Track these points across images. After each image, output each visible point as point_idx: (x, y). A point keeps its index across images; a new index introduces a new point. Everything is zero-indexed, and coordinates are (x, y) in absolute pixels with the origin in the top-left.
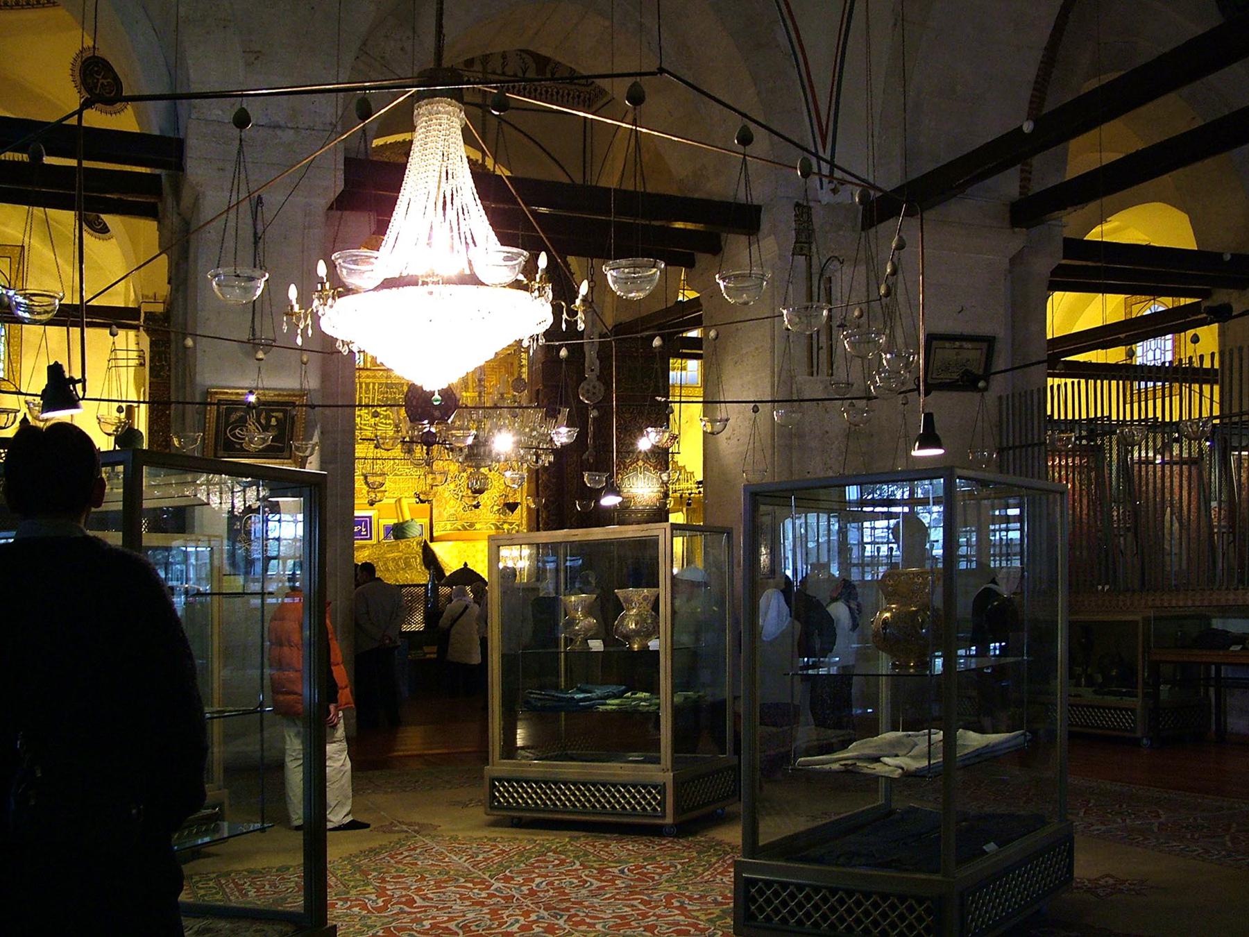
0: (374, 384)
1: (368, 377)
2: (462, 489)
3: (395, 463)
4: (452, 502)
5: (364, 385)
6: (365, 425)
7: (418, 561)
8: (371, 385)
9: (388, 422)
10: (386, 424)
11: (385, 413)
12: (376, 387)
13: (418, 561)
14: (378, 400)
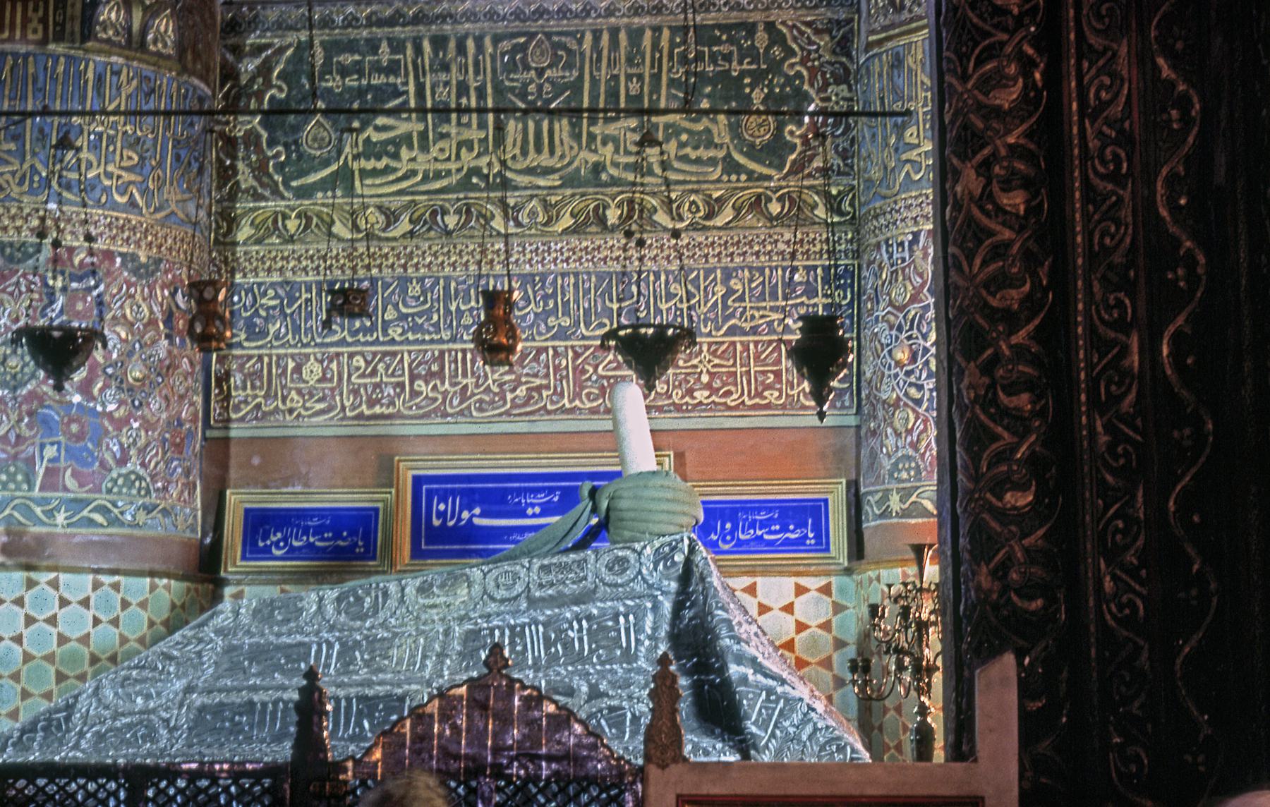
0: (657, 29)
3: (730, 292)
5: (623, 36)
8: (648, 34)
10: (698, 161)
12: (664, 43)
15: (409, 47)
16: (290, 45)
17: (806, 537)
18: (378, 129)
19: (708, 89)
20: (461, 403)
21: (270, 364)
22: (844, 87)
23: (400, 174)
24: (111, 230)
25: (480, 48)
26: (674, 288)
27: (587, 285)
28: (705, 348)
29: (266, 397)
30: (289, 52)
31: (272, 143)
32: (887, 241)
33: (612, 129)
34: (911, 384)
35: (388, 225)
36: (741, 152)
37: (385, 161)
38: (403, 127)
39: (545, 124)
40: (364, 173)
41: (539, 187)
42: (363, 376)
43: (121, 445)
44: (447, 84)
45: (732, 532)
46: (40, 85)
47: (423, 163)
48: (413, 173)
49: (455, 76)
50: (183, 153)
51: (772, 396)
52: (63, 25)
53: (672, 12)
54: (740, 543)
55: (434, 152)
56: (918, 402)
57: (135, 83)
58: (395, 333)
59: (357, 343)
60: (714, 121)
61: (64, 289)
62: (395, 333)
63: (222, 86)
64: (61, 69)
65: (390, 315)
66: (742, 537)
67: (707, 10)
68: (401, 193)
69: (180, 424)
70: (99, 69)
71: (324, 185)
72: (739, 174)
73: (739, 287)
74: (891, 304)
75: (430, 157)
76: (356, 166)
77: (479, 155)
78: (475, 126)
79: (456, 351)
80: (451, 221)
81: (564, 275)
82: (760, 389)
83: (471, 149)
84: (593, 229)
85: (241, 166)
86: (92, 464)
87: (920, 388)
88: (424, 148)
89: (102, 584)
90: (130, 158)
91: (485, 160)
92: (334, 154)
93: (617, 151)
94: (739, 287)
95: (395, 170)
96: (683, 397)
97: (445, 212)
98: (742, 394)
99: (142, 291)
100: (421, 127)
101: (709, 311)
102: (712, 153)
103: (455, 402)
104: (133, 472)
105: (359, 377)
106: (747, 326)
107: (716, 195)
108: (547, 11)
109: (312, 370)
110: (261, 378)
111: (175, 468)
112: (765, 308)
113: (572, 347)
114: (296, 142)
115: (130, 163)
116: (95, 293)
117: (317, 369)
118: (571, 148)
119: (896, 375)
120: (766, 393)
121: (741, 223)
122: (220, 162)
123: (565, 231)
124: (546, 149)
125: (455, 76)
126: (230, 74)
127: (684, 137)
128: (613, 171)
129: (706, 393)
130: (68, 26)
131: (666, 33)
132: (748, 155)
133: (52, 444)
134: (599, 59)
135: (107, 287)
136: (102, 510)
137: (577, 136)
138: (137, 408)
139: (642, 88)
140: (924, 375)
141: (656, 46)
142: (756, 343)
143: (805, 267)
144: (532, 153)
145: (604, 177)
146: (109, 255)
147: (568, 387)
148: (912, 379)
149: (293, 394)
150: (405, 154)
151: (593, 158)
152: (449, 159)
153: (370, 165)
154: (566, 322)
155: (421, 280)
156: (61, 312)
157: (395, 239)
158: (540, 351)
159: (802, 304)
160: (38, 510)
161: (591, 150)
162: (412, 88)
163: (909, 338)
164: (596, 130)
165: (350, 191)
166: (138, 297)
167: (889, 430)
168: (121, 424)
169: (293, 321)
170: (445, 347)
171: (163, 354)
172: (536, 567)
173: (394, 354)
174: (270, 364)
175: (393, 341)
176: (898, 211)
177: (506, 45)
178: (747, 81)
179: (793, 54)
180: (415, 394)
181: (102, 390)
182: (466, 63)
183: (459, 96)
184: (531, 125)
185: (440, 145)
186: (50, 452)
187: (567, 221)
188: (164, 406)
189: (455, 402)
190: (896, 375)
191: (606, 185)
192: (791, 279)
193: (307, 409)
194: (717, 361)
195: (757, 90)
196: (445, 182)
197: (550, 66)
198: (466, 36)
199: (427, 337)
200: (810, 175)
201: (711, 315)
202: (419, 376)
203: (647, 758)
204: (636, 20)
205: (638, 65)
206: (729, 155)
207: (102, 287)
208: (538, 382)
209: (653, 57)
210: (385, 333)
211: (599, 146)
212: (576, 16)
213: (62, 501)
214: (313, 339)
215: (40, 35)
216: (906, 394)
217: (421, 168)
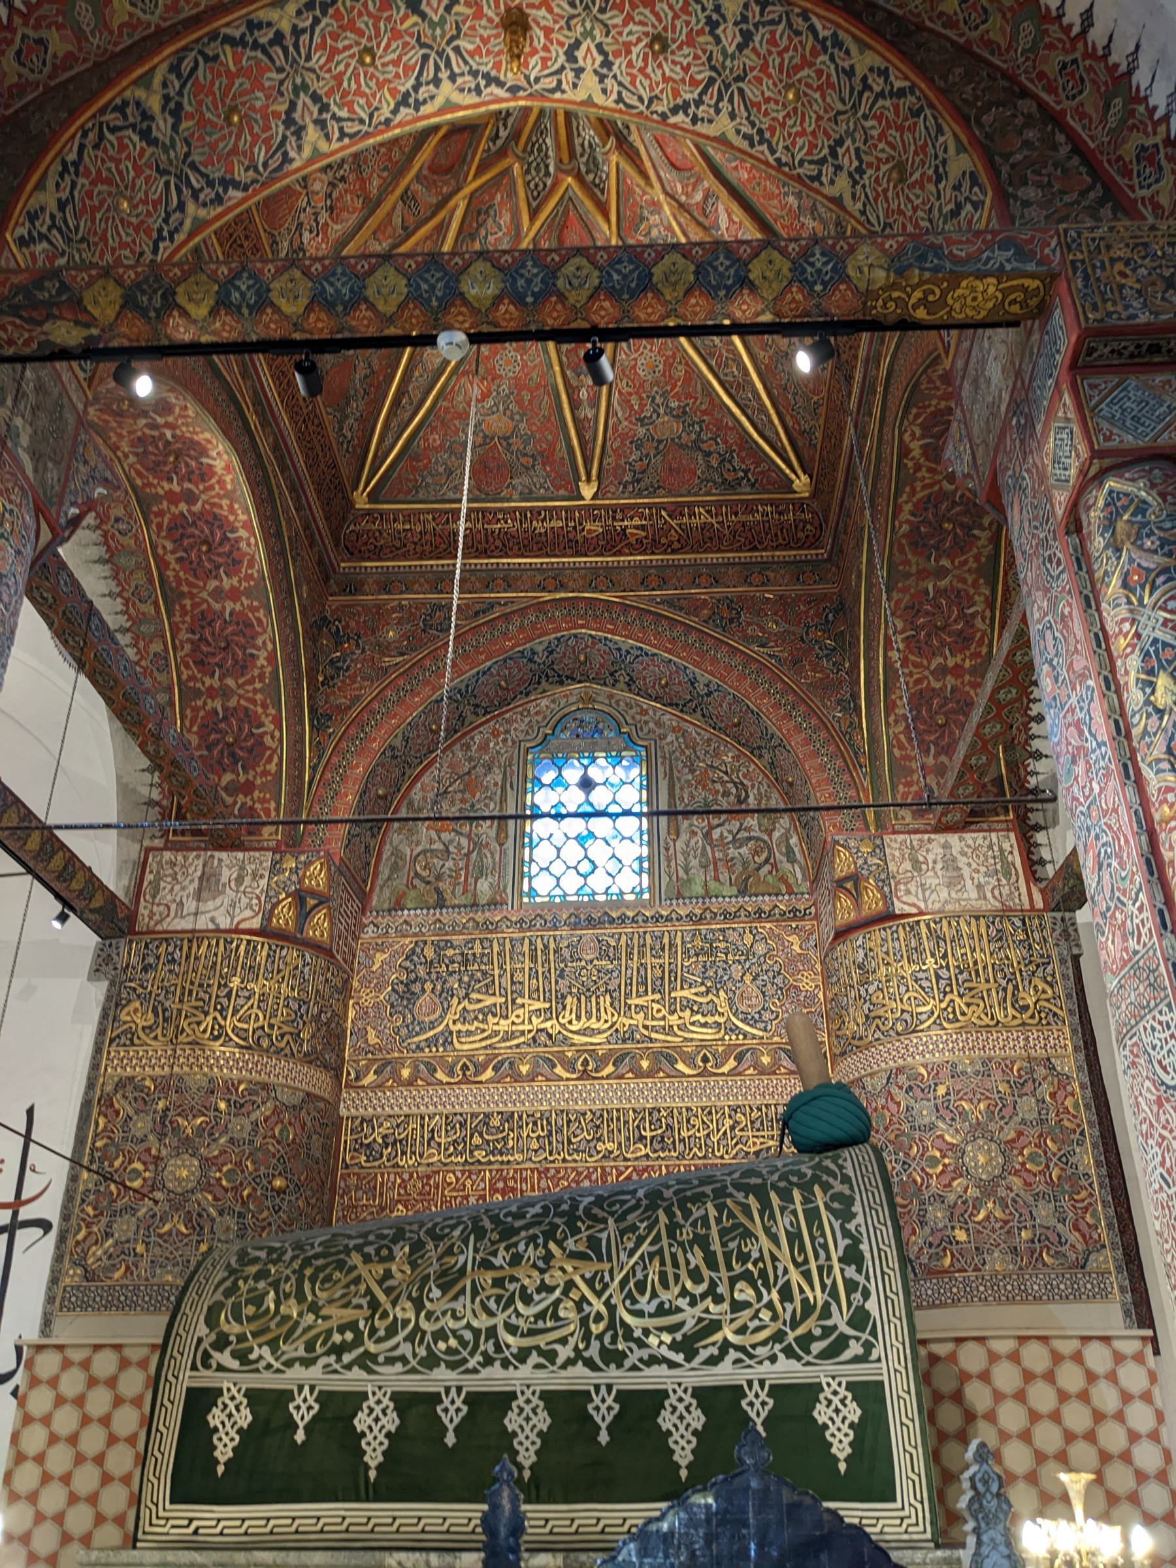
9: (710, 1020)
10: (705, 1025)
38: (489, 1001)
42: (454, 1190)
47: (504, 1025)
55: (513, 1018)
65: (477, 1140)
68: (485, 1048)
77: (546, 1020)
95: (484, 1031)
102: (717, 1018)
123: (608, 1077)
132: (744, 1021)
144: (583, 1019)
151: (628, 1022)
153: (467, 1027)
206: (729, 1019)
210: (472, 1156)
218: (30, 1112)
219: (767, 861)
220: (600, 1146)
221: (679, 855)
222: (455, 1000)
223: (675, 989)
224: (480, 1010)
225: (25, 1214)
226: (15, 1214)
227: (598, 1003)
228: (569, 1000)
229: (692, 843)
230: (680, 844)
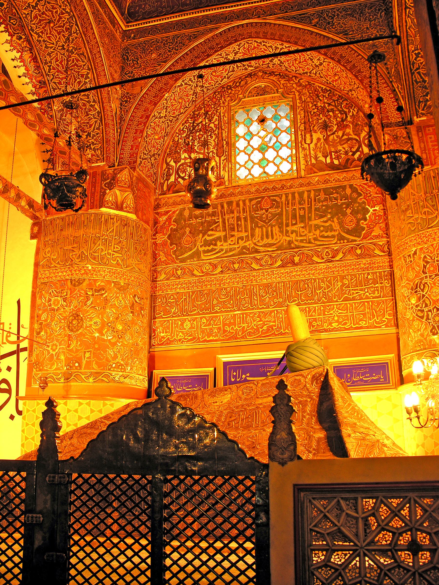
0: (309, 191)
1: (301, 185)
2: (428, 302)
4: (416, 323)
6: (302, 241)
7: (308, 409)
8: (306, 193)
11: (327, 224)
12: (312, 195)
13: (308, 409)
14: (316, 209)
15: (219, 206)
16: (177, 210)
17: (380, 378)
18: (209, 236)
19: (330, 211)
20: (242, 334)
21: (172, 323)
22: (381, 205)
23: (217, 251)
24: (110, 273)
25: (244, 204)
26: (322, 285)
27: (288, 286)
28: (335, 307)
29: (171, 335)
30: (177, 212)
31: (171, 245)
32: (403, 256)
33: (294, 228)
34: (419, 310)
35: (213, 269)
36: (344, 232)
37: (212, 246)
38: (218, 234)
39: (270, 229)
40: (205, 252)
41: (269, 251)
43: (114, 352)
44: (233, 217)
45: (350, 378)
46: (85, 224)
47: (226, 246)
48: (222, 250)
49: (236, 214)
50: (138, 247)
51: (363, 323)
52: (93, 203)
53: (314, 185)
54: (354, 382)
55: (229, 242)
56: (422, 317)
57: (119, 222)
58: (217, 309)
59: (204, 314)
60: (333, 221)
61: (93, 295)
62: (217, 309)
63: (154, 226)
64: (92, 218)
65: (215, 302)
66: (354, 379)
67: (327, 183)
68: (217, 258)
69: (138, 345)
70: (106, 218)
71: (191, 257)
72: (343, 240)
73: (347, 282)
74: (407, 280)
75: (228, 244)
76: (201, 249)
77: (245, 242)
78: (244, 231)
79: (240, 314)
80: (236, 266)
81: (279, 283)
82: (358, 321)
83: (243, 240)
84: (289, 265)
85: (161, 253)
86: (103, 359)
87: (422, 311)
88: (226, 241)
89: (107, 404)
90: (117, 248)
91: (248, 243)
92: (194, 246)
93: (297, 236)
94: (347, 282)
95: (215, 249)
96: (328, 326)
97: (234, 263)
98: (351, 323)
99: (122, 295)
100: (224, 233)
101: (336, 292)
102: (333, 233)
103: (240, 333)
104: (118, 362)
105: (204, 326)
106: (351, 297)
107: (335, 248)
108: (269, 189)
109: (187, 325)
110: (169, 328)
111: (135, 362)
112: (357, 290)
113: (284, 310)
114: (180, 243)
115: (117, 250)
116: (104, 296)
117: (189, 324)
118: (280, 236)
119: (412, 308)
120: (360, 323)
121: (346, 258)
122: (154, 252)
123: (279, 267)
124: (270, 237)
125: (236, 214)
126: (156, 222)
127: (322, 228)
128: (296, 243)
129: (337, 324)
130: (95, 203)
131: (313, 192)
132: (347, 233)
133: (88, 352)
134: (288, 204)
135: (108, 294)
136: (107, 376)
137: (281, 232)
138: (120, 338)
139: (305, 212)
140: (424, 306)
141: (309, 197)
142: (355, 303)
143: (372, 273)
144: (265, 239)
145: (292, 245)
146: (109, 282)
147: (283, 325)
148: (419, 308)
149: (181, 334)
150: (219, 243)
151: (288, 239)
152: (235, 244)
153: (207, 248)
154: (281, 300)
155: (225, 289)
156: (92, 303)
157: (216, 274)
158: (271, 312)
159: (372, 287)
160: (83, 376)
161: (287, 236)
162: (220, 220)
163: (416, 292)
164: (288, 229)
165: (199, 259)
166: (121, 298)
167: (411, 331)
168: (114, 344)
169: (180, 307)
170: (235, 313)
171: (130, 319)
172: (260, 385)
173: (217, 317)
174: (172, 323)
175: (217, 312)
176: (407, 243)
177: (254, 202)
178: (344, 206)
179: (361, 195)
180: (225, 331)
181: (106, 332)
182: (240, 210)
183: (237, 221)
184: (264, 229)
185: (231, 239)
186: (87, 355)
187: (279, 263)
188: (131, 338)
189: (240, 333)
190: (412, 308)
191: (294, 248)
192: (367, 278)
193: (186, 339)
194: (340, 311)
195: (348, 209)
196: (233, 252)
197: (270, 208)
198: (239, 200)
199: (229, 309)
200: (371, 239)
201: (337, 294)
202: (226, 324)
203: (271, 457)
204: (301, 188)
205: (303, 204)
206: (340, 233)
207: (106, 294)
208: (272, 324)
209: (308, 201)
211: (290, 234)
212: (279, 189)
213: (91, 373)
214: (187, 313)
215: (86, 207)
216: (417, 315)
217: (224, 248)
218: (19, 302)
219: (357, 150)
220: (275, 300)
221: (312, 152)
222: (201, 235)
223: (311, 220)
224: (213, 240)
225: (22, 345)
226: (18, 346)
227: (272, 231)
228: (257, 229)
229: (319, 144)
230: (312, 146)
